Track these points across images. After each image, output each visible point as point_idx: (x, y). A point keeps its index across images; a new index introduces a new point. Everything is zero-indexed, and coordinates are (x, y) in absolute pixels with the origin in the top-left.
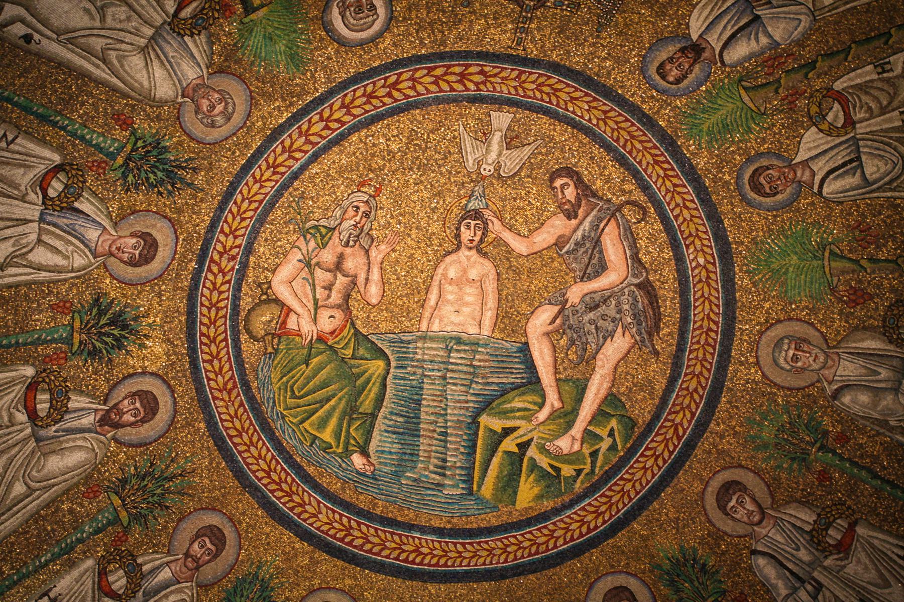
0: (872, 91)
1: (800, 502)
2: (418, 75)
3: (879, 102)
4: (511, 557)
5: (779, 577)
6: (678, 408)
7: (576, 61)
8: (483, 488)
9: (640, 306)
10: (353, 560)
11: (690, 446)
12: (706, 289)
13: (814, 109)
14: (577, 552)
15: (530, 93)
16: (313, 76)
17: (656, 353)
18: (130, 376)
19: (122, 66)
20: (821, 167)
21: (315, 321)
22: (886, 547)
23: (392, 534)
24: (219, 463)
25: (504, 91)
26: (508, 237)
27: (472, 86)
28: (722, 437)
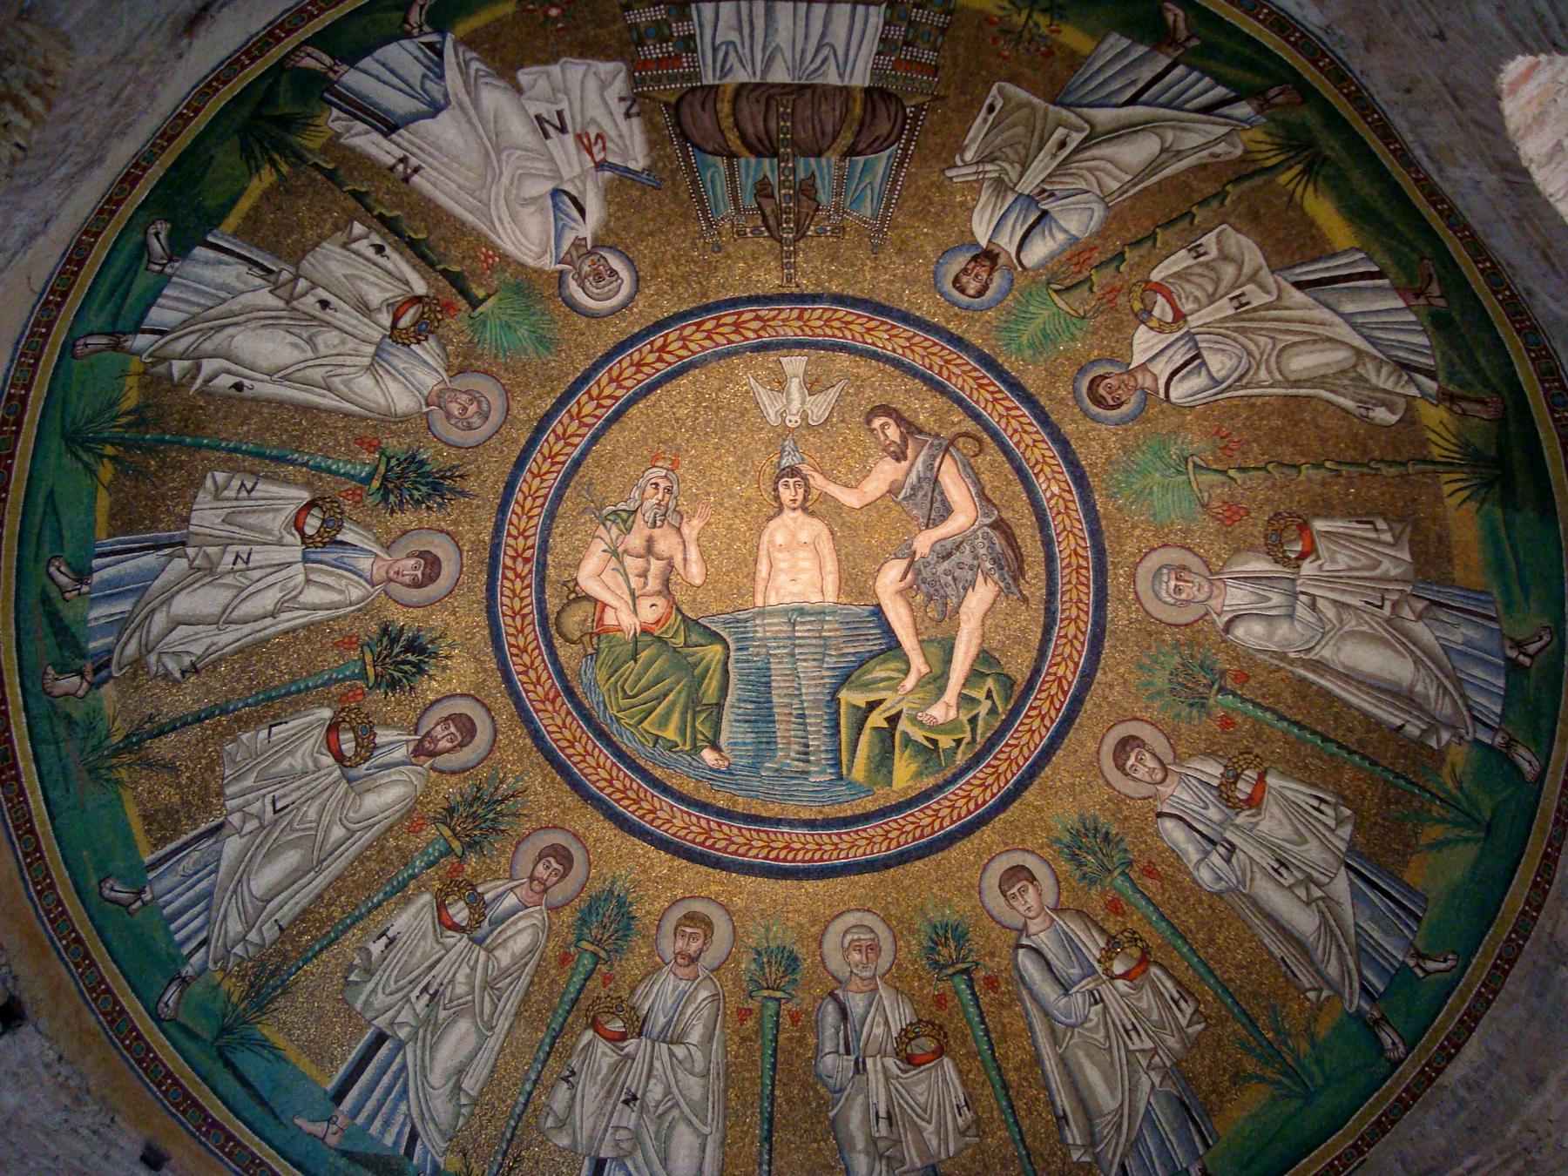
0: (1194, 278)
1: (1205, 754)
2: (686, 332)
3: (1204, 290)
4: (894, 843)
5: (1189, 841)
6: (1059, 659)
8: (854, 771)
9: (998, 547)
10: (718, 864)
11: (1077, 701)
12: (1067, 522)
13: (1137, 306)
14: (967, 830)
15: (818, 331)
16: (568, 356)
17: (1025, 600)
18: (438, 701)
19: (350, 389)
20: (1162, 369)
21: (635, 612)
22: (1301, 800)
23: (758, 831)
24: (553, 780)
25: (789, 333)
26: (834, 490)
27: (751, 335)
28: (1111, 686)
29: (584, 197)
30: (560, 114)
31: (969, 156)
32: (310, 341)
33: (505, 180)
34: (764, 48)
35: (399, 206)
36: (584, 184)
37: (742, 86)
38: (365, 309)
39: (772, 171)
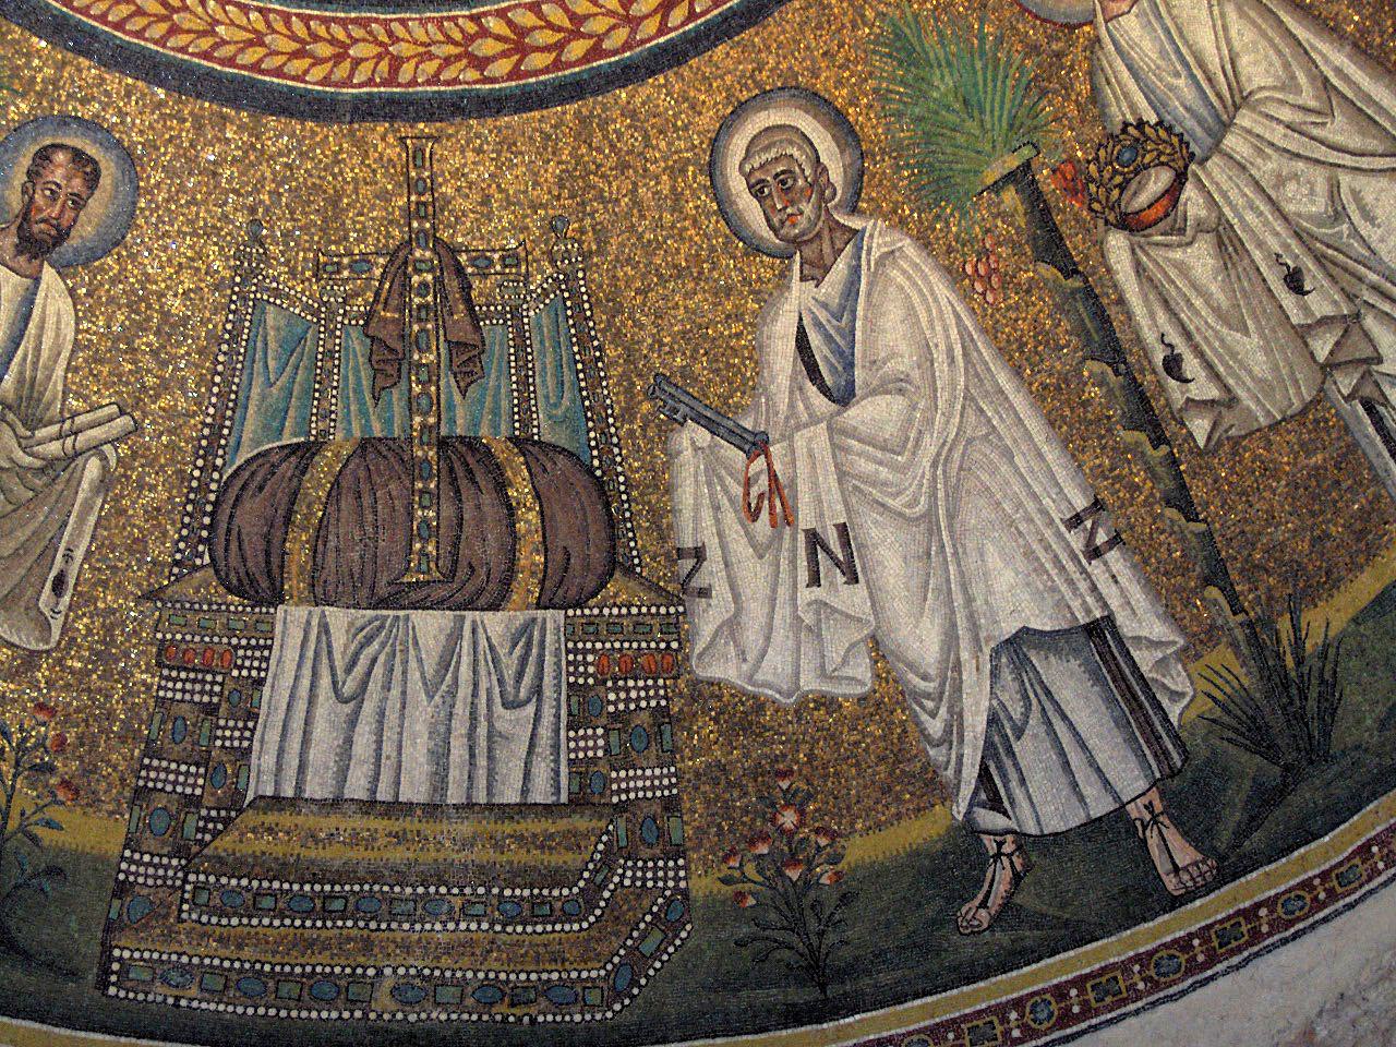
2: (622, 34)
7: (278, 134)
15: (358, 32)
19: (1286, 66)
27: (493, 24)
29: (793, 378)
30: (815, 580)
31: (93, 468)
32: (1338, 215)
33: (930, 447)
34: (452, 692)
35: (1120, 451)
36: (792, 406)
37: (494, 607)
38: (1227, 243)
39: (451, 407)
